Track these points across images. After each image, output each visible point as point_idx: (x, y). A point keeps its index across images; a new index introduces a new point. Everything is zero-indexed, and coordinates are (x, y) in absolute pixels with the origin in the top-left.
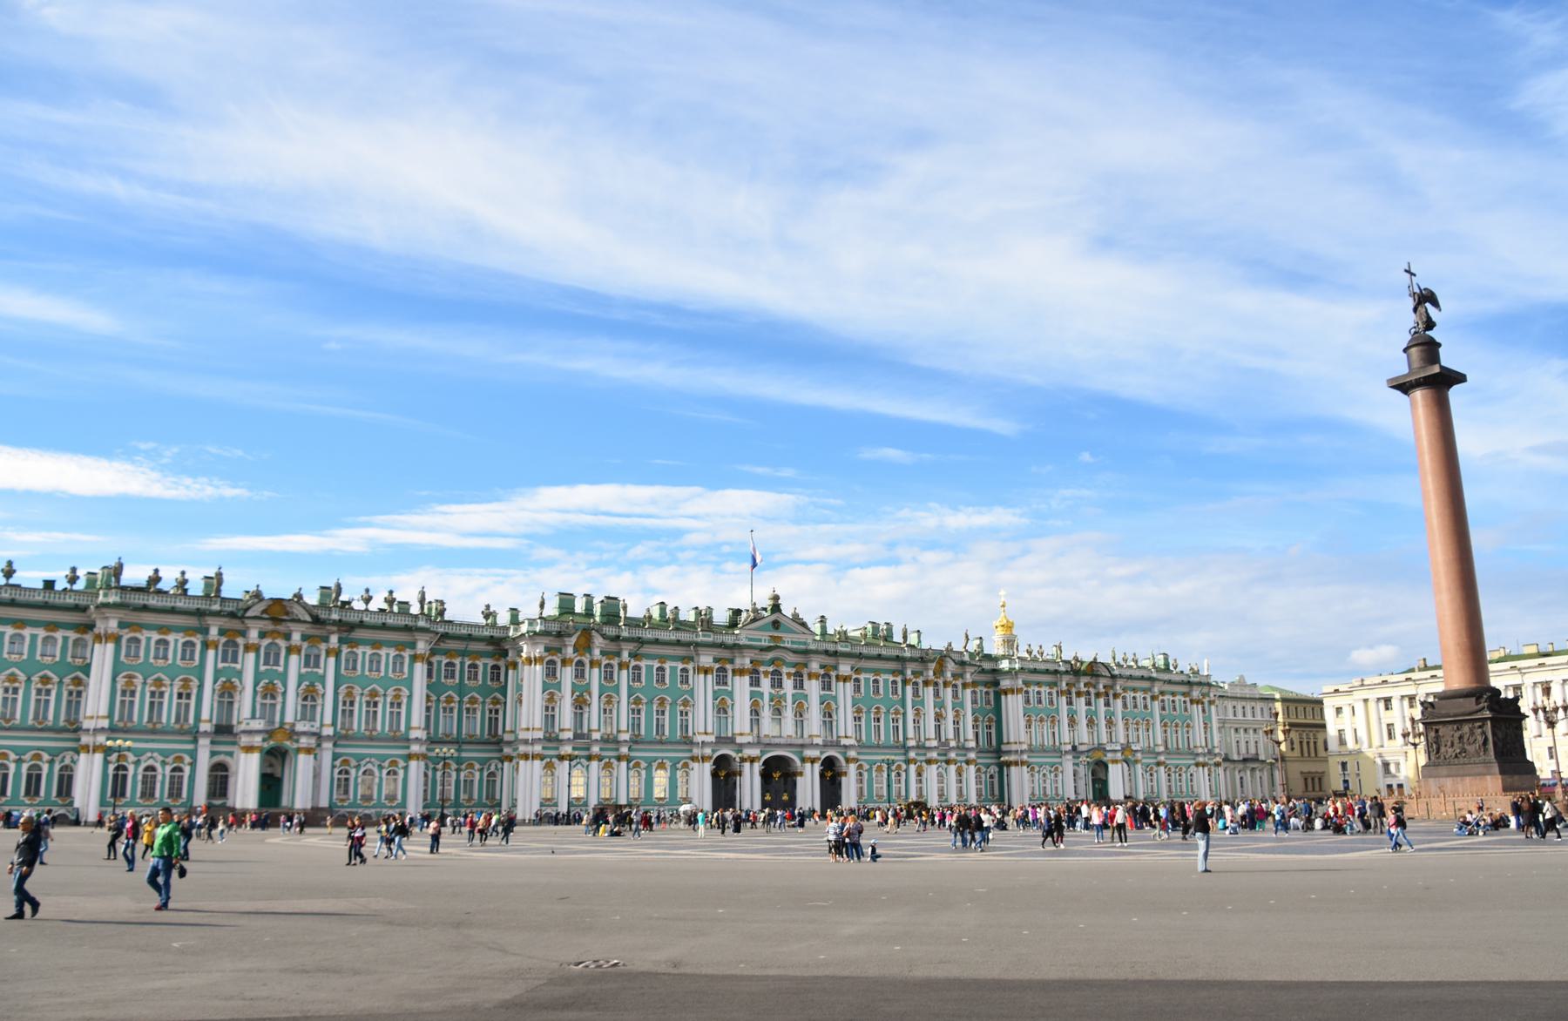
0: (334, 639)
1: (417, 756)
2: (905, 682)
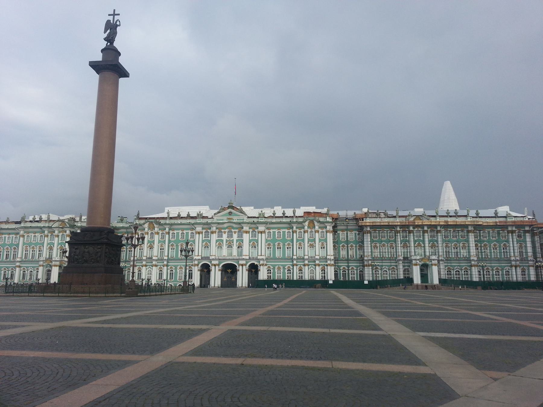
2: (293, 232)
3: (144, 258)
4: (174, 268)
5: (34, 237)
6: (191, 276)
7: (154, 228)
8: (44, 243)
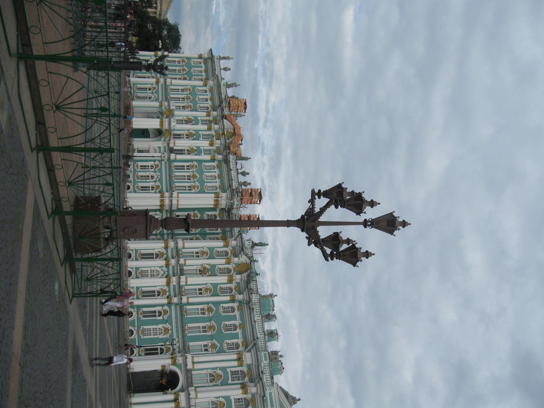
0: (220, 157)
1: (162, 196)
3: (182, 261)
4: (166, 317)
5: (205, 99)
6: (151, 352)
7: (239, 273)
8: (198, 111)
